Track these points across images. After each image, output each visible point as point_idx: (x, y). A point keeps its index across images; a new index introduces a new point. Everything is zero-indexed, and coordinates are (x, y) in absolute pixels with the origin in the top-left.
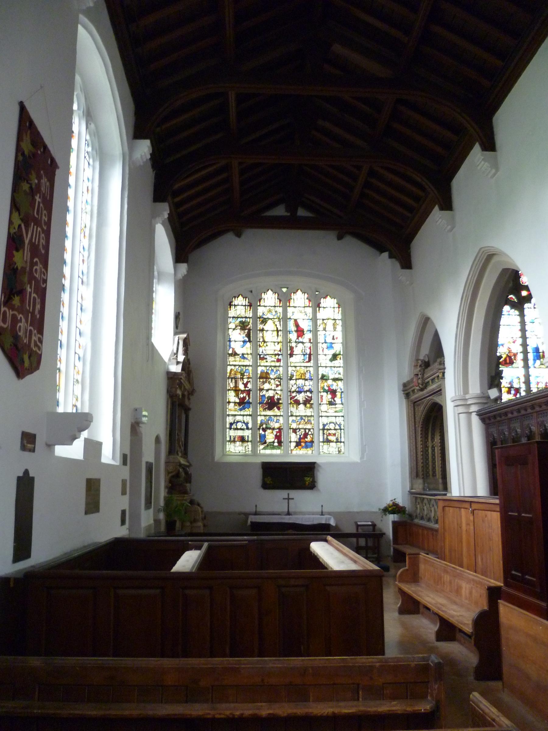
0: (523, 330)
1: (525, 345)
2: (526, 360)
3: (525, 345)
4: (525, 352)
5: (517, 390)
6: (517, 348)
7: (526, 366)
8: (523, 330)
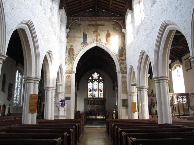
0: (93, 86)
1: (93, 88)
2: (93, 91)
3: (93, 88)
4: (93, 90)
5: (91, 96)
6: (92, 89)
7: (93, 92)
8: (93, 86)
